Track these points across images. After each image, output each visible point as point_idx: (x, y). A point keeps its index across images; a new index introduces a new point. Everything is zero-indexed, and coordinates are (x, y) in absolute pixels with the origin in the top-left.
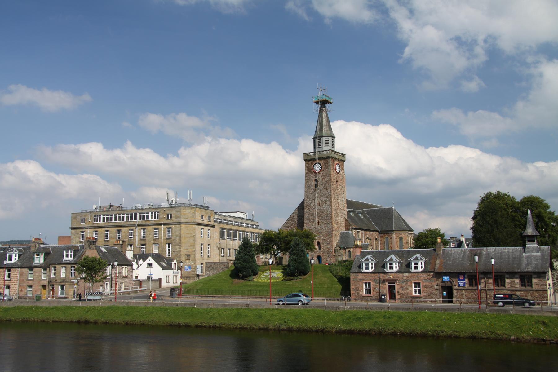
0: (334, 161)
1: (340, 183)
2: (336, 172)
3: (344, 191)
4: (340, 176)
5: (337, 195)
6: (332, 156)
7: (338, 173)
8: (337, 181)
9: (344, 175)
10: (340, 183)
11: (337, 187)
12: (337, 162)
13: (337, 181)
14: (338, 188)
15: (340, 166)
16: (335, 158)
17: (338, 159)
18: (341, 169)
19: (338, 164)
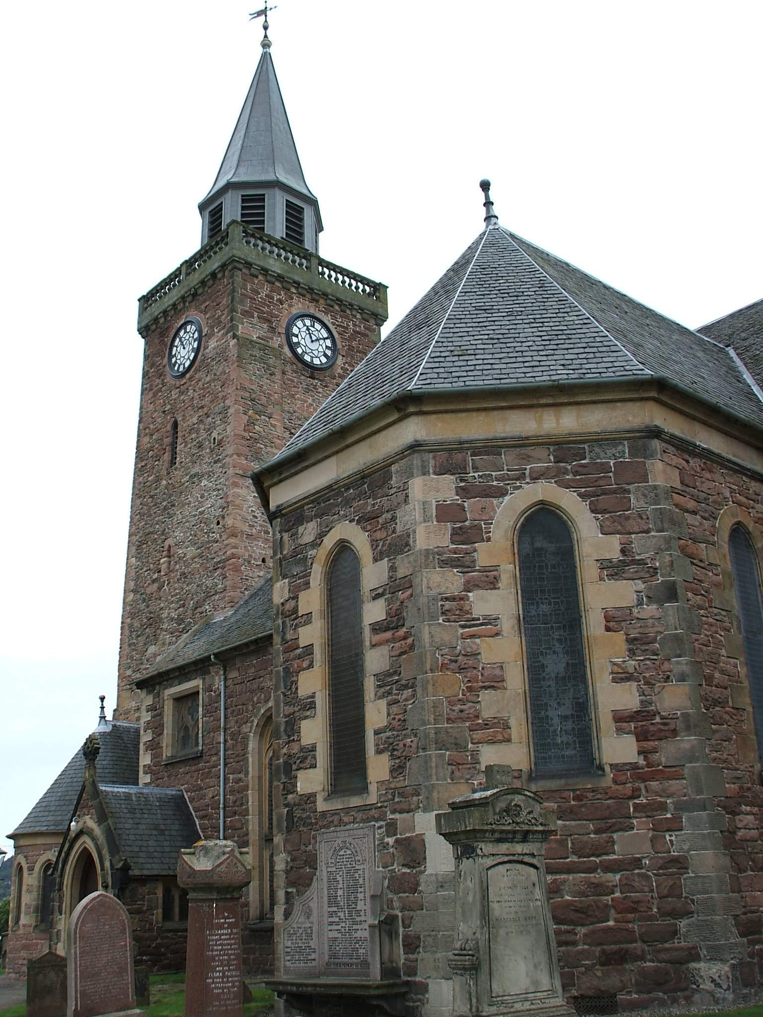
3: (220, 443)
5: (165, 508)
7: (183, 375)
9: (233, 342)
13: (175, 425)
16: (165, 312)
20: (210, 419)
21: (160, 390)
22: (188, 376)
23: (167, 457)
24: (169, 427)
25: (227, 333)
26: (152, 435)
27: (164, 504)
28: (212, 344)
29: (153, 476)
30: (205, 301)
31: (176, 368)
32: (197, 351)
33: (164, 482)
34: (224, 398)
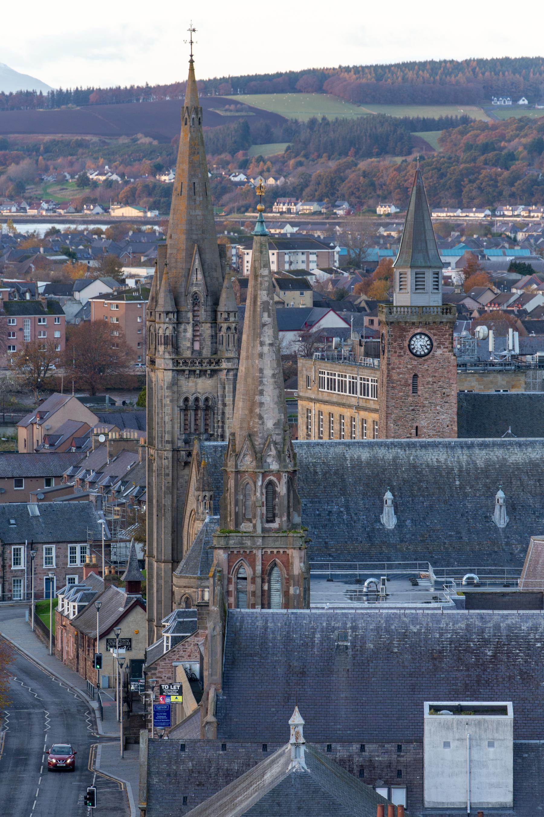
0: (404, 330)
1: (430, 379)
2: (415, 355)
3: (448, 396)
4: (430, 362)
5: (413, 410)
6: (391, 321)
7: (420, 356)
8: (415, 376)
10: (430, 379)
11: (415, 390)
12: (419, 331)
13: (415, 376)
14: (419, 393)
15: (434, 338)
16: (406, 323)
17: (420, 322)
18: (435, 344)
19: (421, 334)
20: (440, 383)
21: (402, 356)
22: (423, 358)
23: (411, 388)
24: (412, 375)
25: (449, 352)
26: (399, 374)
27: (412, 408)
28: (439, 352)
29: (402, 394)
30: (433, 329)
31: (415, 351)
32: (430, 351)
33: (410, 398)
34: (450, 379)
